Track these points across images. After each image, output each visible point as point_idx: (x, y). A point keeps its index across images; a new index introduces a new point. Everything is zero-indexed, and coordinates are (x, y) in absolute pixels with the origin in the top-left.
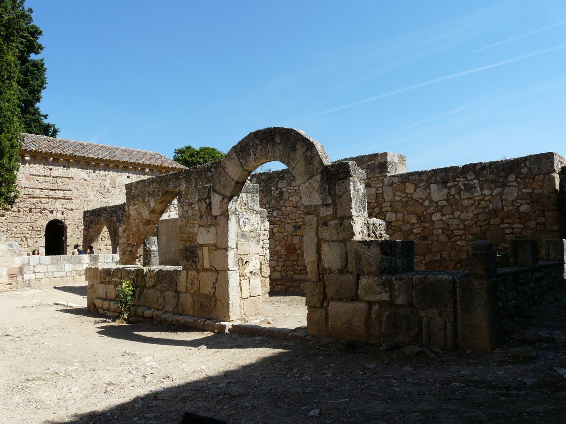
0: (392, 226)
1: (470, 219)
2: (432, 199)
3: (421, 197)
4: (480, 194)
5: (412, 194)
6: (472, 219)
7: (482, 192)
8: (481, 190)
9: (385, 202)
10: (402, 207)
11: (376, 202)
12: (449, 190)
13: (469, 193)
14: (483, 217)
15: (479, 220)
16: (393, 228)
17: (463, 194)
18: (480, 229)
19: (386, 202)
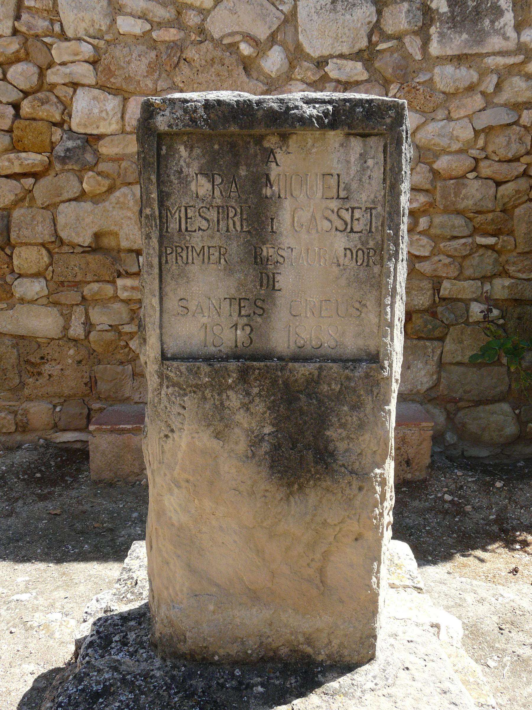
0: (99, 157)
1: (455, 147)
2: (298, 47)
3: (245, 28)
4: (511, 45)
5: (204, 13)
6: (461, 151)
7: (519, 38)
8: (518, 27)
9: (63, 36)
10: (151, 68)
11: (15, 32)
12: (379, 12)
13: (465, 36)
14: (509, 143)
15: (487, 158)
16: (102, 167)
17: (442, 35)
18: (493, 190)
19: (67, 39)
